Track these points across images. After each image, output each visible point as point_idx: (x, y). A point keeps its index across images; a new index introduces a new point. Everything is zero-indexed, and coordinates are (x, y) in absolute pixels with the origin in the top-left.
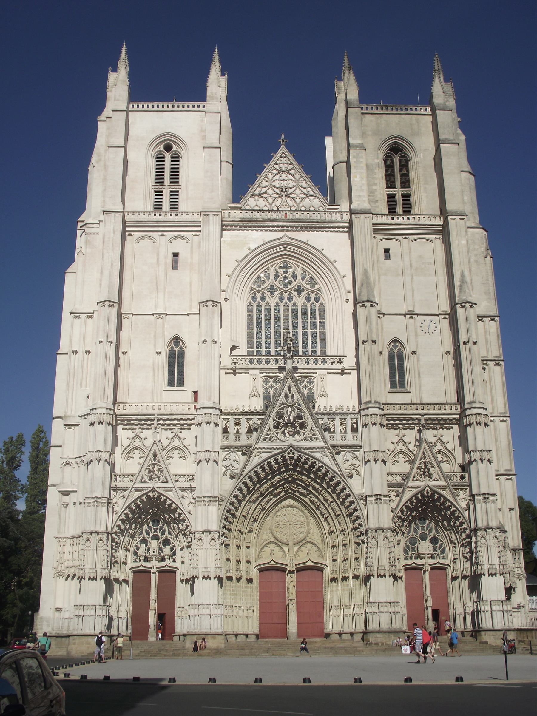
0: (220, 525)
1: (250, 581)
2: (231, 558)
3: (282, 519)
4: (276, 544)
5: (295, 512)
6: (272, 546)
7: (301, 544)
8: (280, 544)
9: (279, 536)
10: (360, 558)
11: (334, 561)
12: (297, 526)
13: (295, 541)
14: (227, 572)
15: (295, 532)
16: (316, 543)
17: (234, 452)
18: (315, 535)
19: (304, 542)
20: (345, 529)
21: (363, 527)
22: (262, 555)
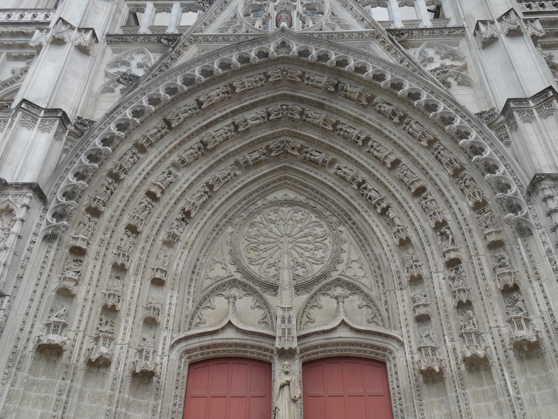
0: (58, 185)
1: (144, 378)
2: (81, 292)
3: (265, 231)
4: (244, 286)
5: (299, 216)
6: (235, 291)
7: (316, 288)
8: (258, 288)
9: (254, 269)
10: (523, 284)
11: (423, 319)
12: (305, 245)
13: (300, 281)
14: (48, 332)
15: (300, 260)
16: (357, 284)
17: (143, 52)
18: (355, 265)
19: (325, 282)
20: (445, 223)
21: (514, 188)
22: (204, 317)
